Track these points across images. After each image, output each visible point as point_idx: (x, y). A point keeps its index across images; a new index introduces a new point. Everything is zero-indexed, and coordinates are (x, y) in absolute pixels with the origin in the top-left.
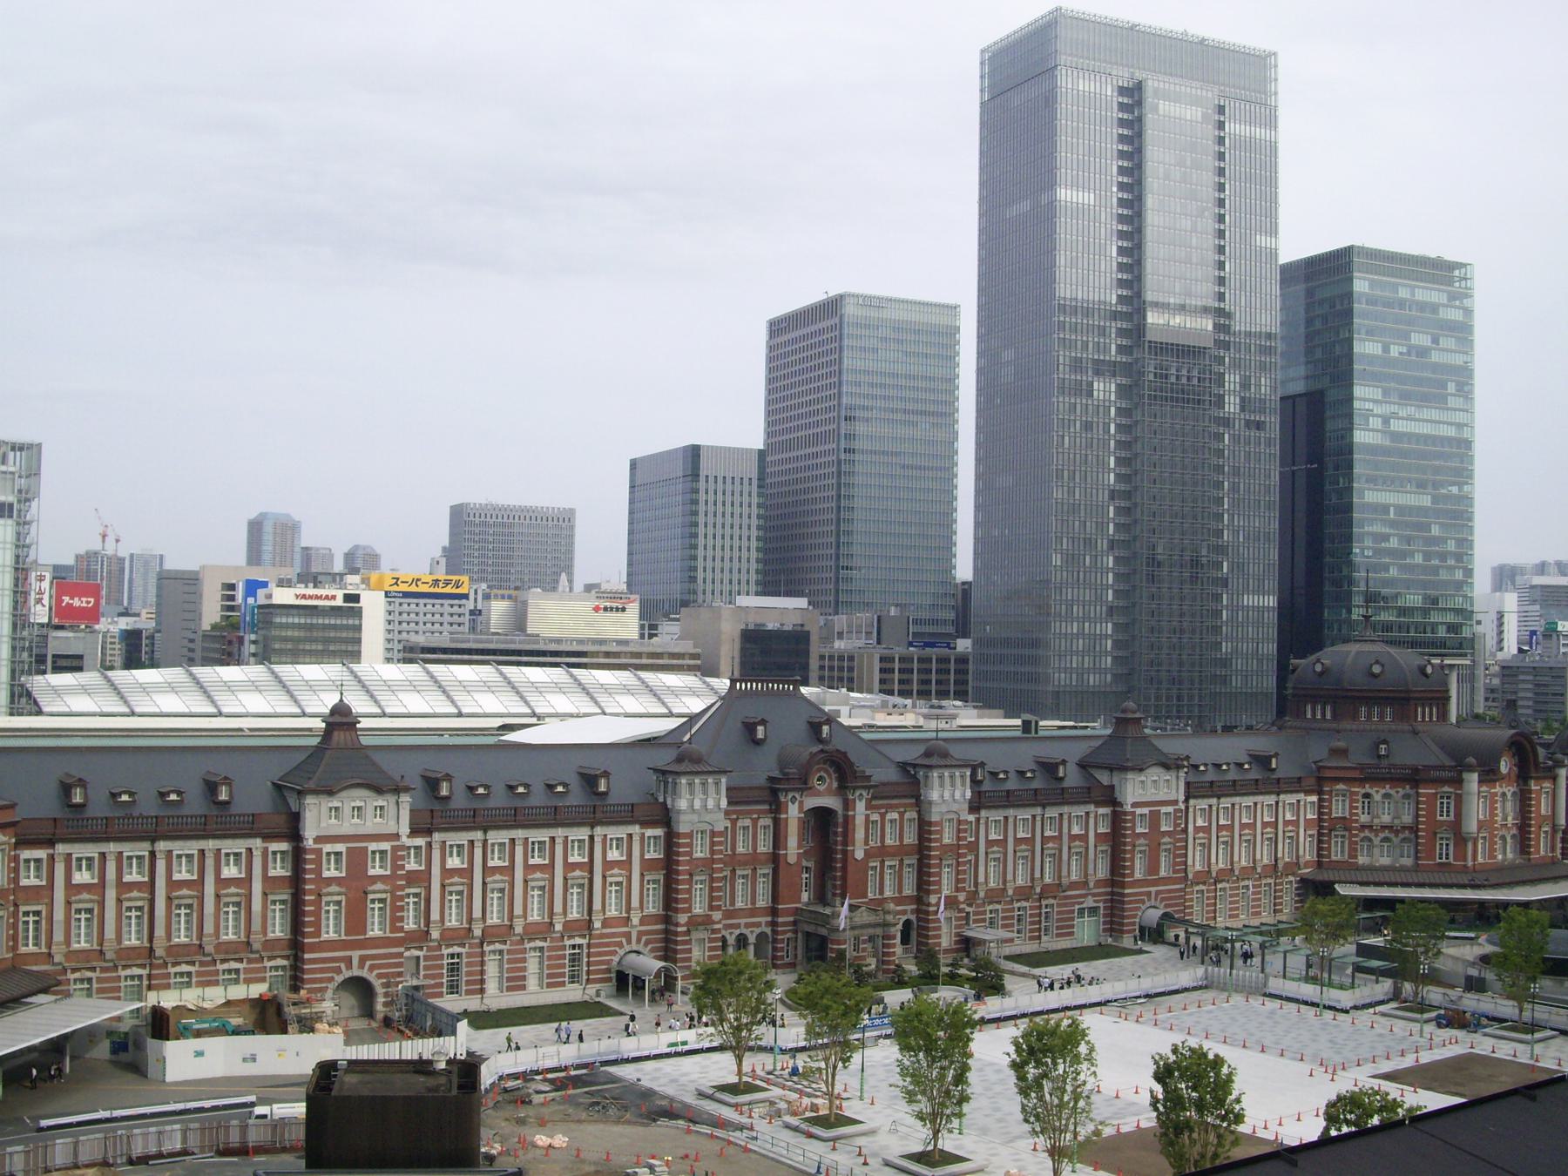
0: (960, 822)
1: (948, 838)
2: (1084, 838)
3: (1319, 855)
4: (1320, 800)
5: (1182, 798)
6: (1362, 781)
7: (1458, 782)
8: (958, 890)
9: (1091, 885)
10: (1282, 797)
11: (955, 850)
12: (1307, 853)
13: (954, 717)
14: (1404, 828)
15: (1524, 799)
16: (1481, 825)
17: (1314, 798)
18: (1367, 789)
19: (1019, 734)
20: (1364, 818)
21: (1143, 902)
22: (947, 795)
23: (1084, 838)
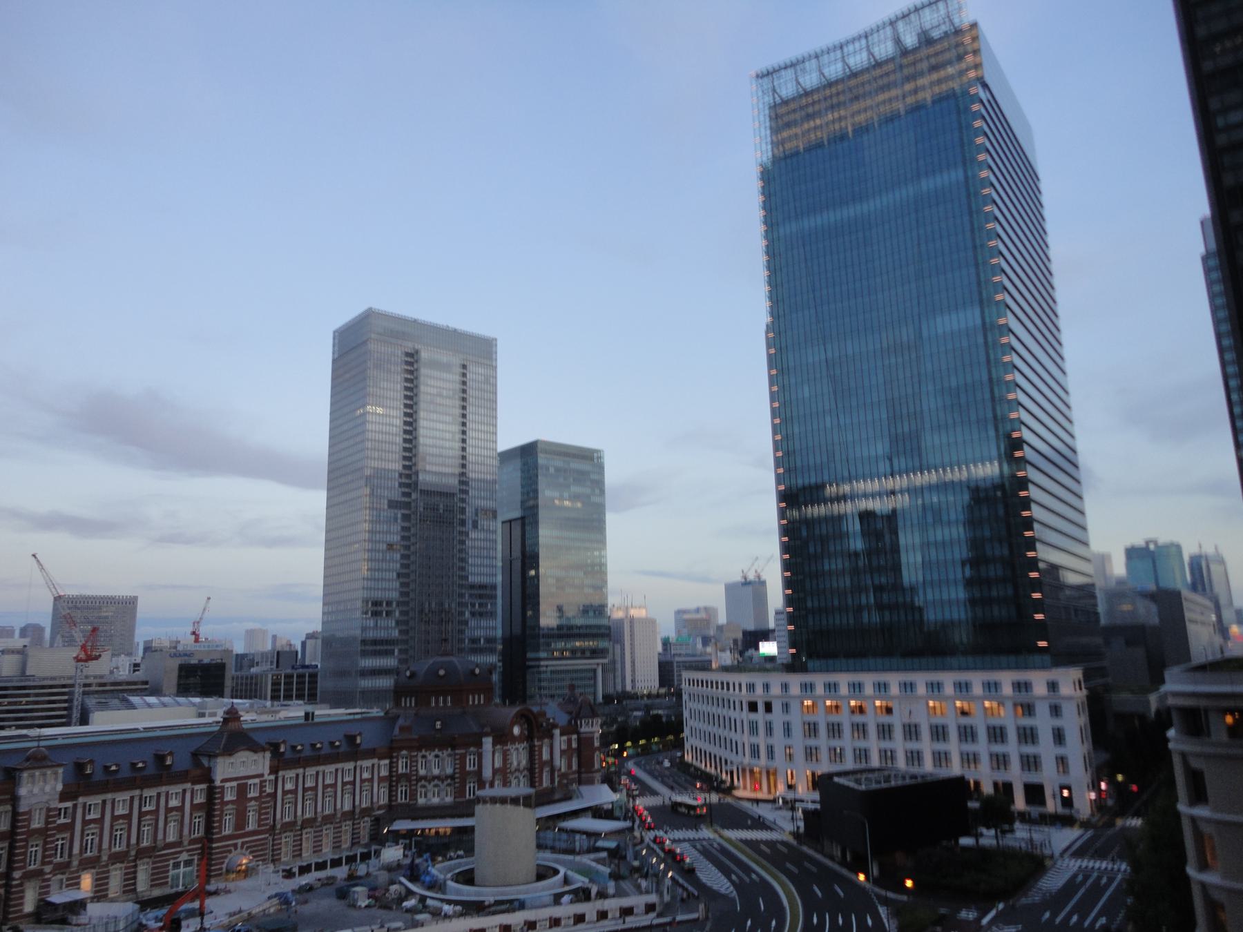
0: (49, 810)
1: (36, 824)
2: (181, 809)
3: (390, 800)
4: (391, 763)
5: (267, 771)
6: (419, 749)
7: (479, 745)
8: (43, 863)
9: (186, 843)
10: (359, 763)
11: (43, 832)
12: (384, 801)
13: (278, 712)
14: (447, 777)
15: (532, 753)
16: (495, 772)
17: (387, 762)
18: (423, 752)
19: (302, 721)
20: (422, 772)
21: (230, 852)
22: (39, 791)
23: (181, 809)
